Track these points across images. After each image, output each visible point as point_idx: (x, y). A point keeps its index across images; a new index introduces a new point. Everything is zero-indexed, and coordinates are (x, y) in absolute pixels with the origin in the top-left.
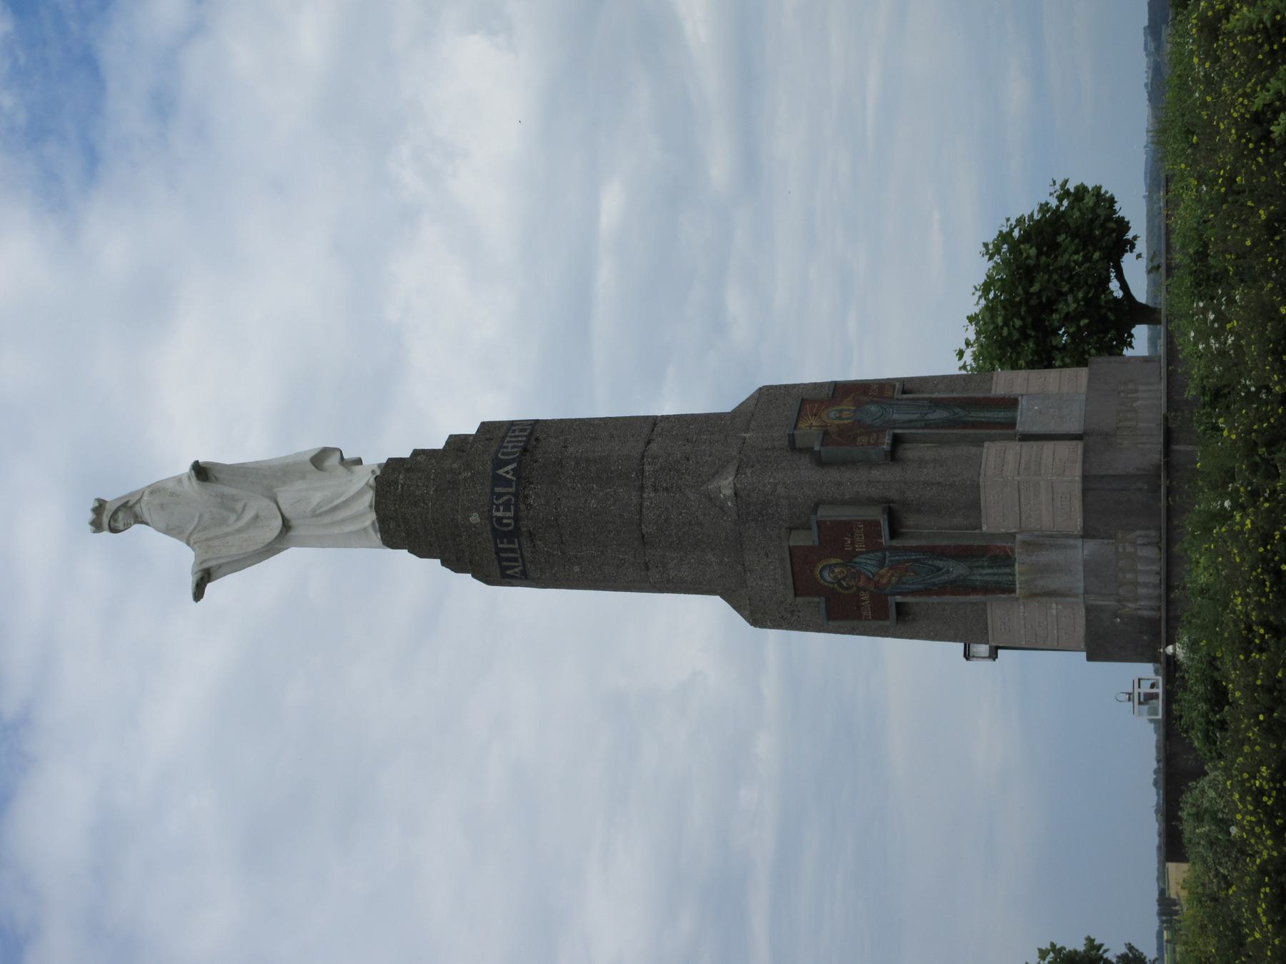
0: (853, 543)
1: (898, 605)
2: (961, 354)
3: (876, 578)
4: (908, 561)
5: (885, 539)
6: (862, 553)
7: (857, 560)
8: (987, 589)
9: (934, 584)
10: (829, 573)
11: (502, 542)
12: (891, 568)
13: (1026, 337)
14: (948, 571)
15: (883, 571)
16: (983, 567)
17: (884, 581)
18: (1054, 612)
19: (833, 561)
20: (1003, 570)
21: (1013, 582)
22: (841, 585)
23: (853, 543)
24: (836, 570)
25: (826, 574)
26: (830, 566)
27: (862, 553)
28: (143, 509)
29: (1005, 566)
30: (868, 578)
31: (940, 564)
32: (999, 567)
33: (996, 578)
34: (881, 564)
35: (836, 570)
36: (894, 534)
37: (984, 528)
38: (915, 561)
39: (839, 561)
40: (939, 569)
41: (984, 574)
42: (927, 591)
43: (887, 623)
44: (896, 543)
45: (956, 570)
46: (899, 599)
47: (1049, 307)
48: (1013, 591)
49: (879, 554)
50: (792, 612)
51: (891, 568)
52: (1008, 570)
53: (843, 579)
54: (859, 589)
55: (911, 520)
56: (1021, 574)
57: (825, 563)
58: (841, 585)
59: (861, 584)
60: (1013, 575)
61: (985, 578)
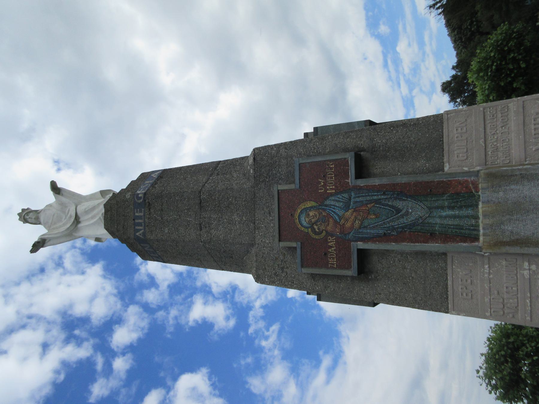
0: (325, 185)
1: (361, 252)
2: (478, 372)
3: (342, 221)
4: (371, 202)
5: (351, 180)
6: (332, 195)
7: (328, 202)
8: (447, 236)
9: (393, 229)
10: (305, 217)
11: (137, 212)
12: (355, 210)
13: (507, 362)
14: (407, 213)
15: (348, 214)
16: (443, 208)
17: (348, 225)
18: (526, 273)
19: (309, 204)
20: (464, 212)
21: (476, 228)
22: (313, 230)
23: (325, 185)
24: (311, 214)
25: (303, 219)
26: (306, 209)
27: (332, 195)
28: (42, 218)
29: (467, 207)
30: (335, 222)
31: (399, 204)
32: (461, 208)
33: (456, 222)
34: (347, 207)
35: (311, 214)
36: (359, 176)
37: (446, 169)
38: (377, 202)
39: (313, 204)
40: (398, 211)
41: (444, 217)
42: (385, 237)
43: (349, 273)
44: (361, 183)
45: (415, 211)
46: (361, 245)
47: (517, 349)
48: (476, 239)
49: (346, 195)
50: (282, 268)
51: (355, 210)
52: (470, 212)
53: (315, 223)
54: (328, 234)
55: (378, 167)
56: (485, 216)
57: (302, 206)
58: (313, 230)
59: (329, 228)
60: (477, 218)
61: (445, 222)
